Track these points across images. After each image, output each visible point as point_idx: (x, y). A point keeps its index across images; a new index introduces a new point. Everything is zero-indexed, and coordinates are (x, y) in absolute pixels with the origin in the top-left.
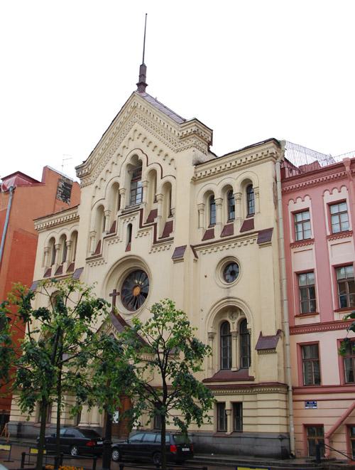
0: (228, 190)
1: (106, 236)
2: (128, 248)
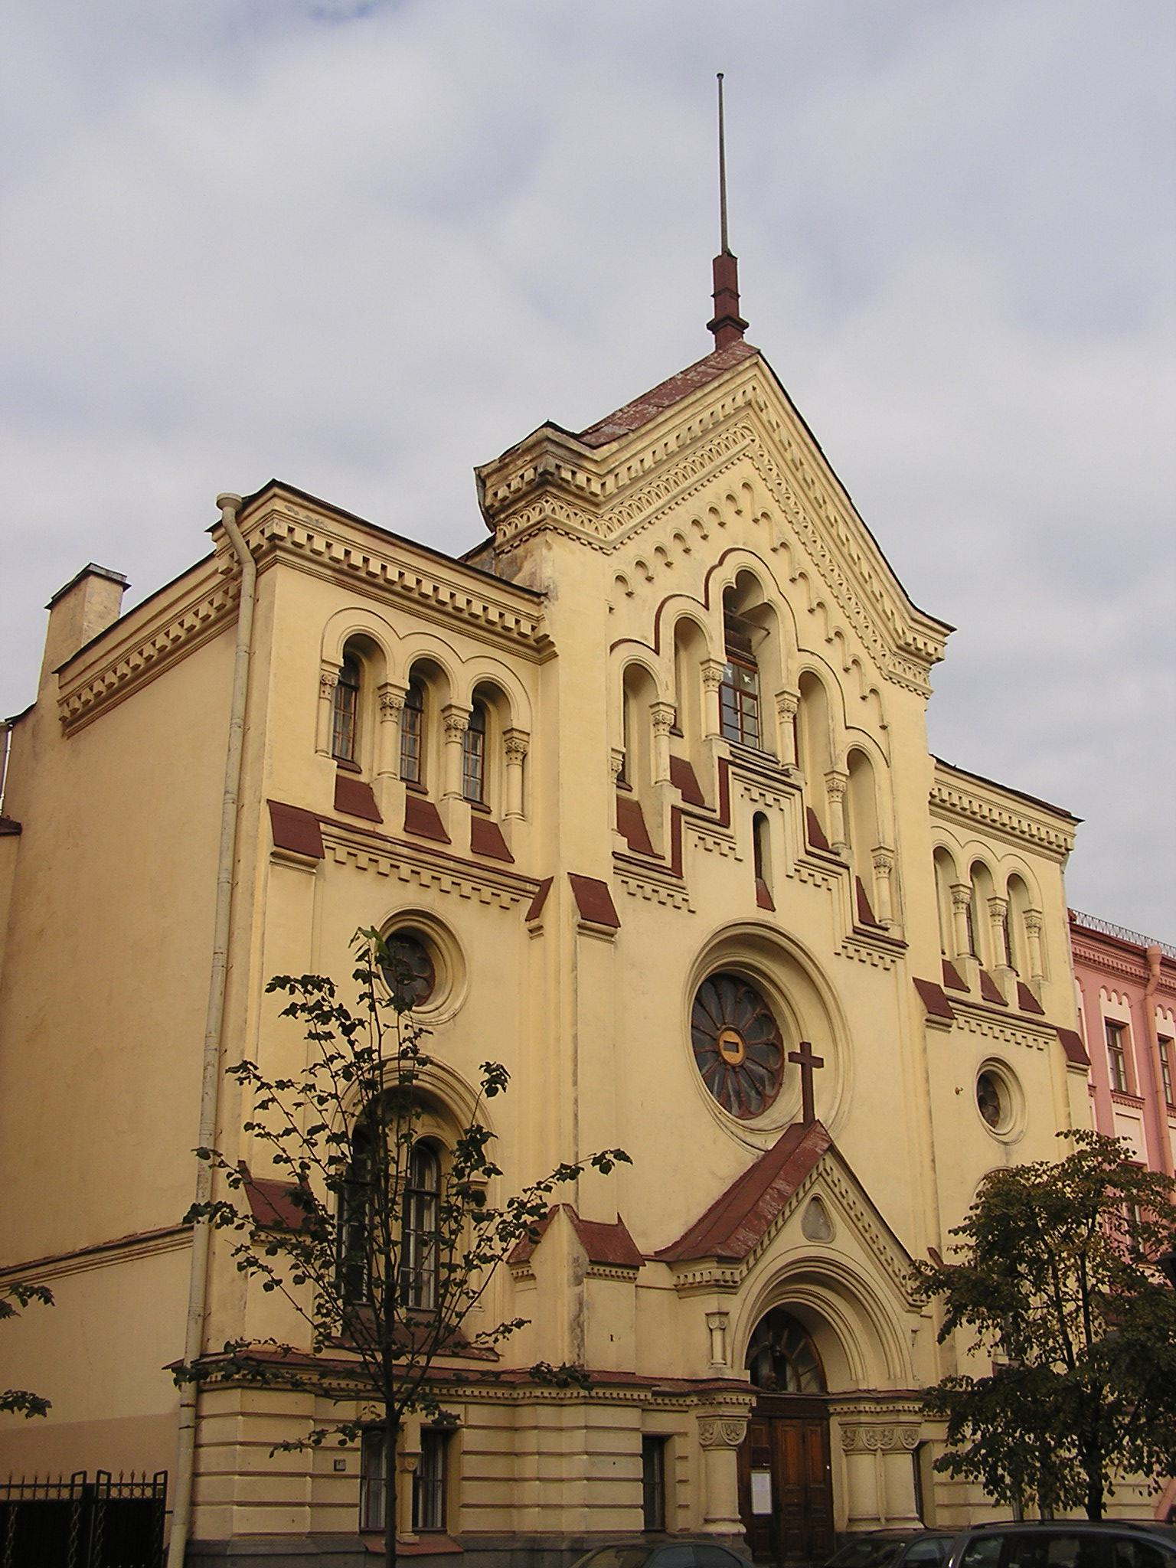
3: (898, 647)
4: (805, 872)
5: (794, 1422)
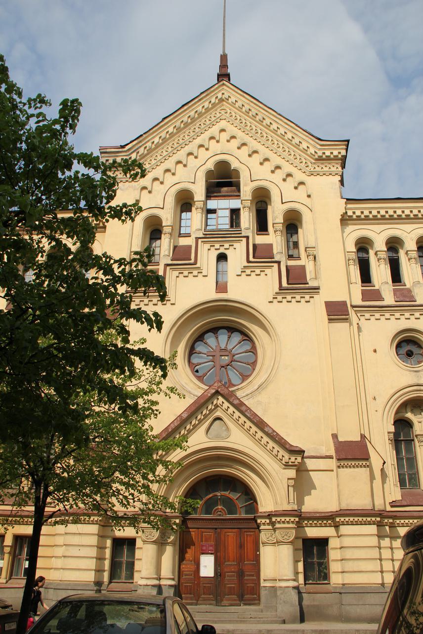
0: (394, 245)
1: (171, 262)
2: (221, 287)
3: (316, 160)
4: (248, 271)
5: (234, 530)
